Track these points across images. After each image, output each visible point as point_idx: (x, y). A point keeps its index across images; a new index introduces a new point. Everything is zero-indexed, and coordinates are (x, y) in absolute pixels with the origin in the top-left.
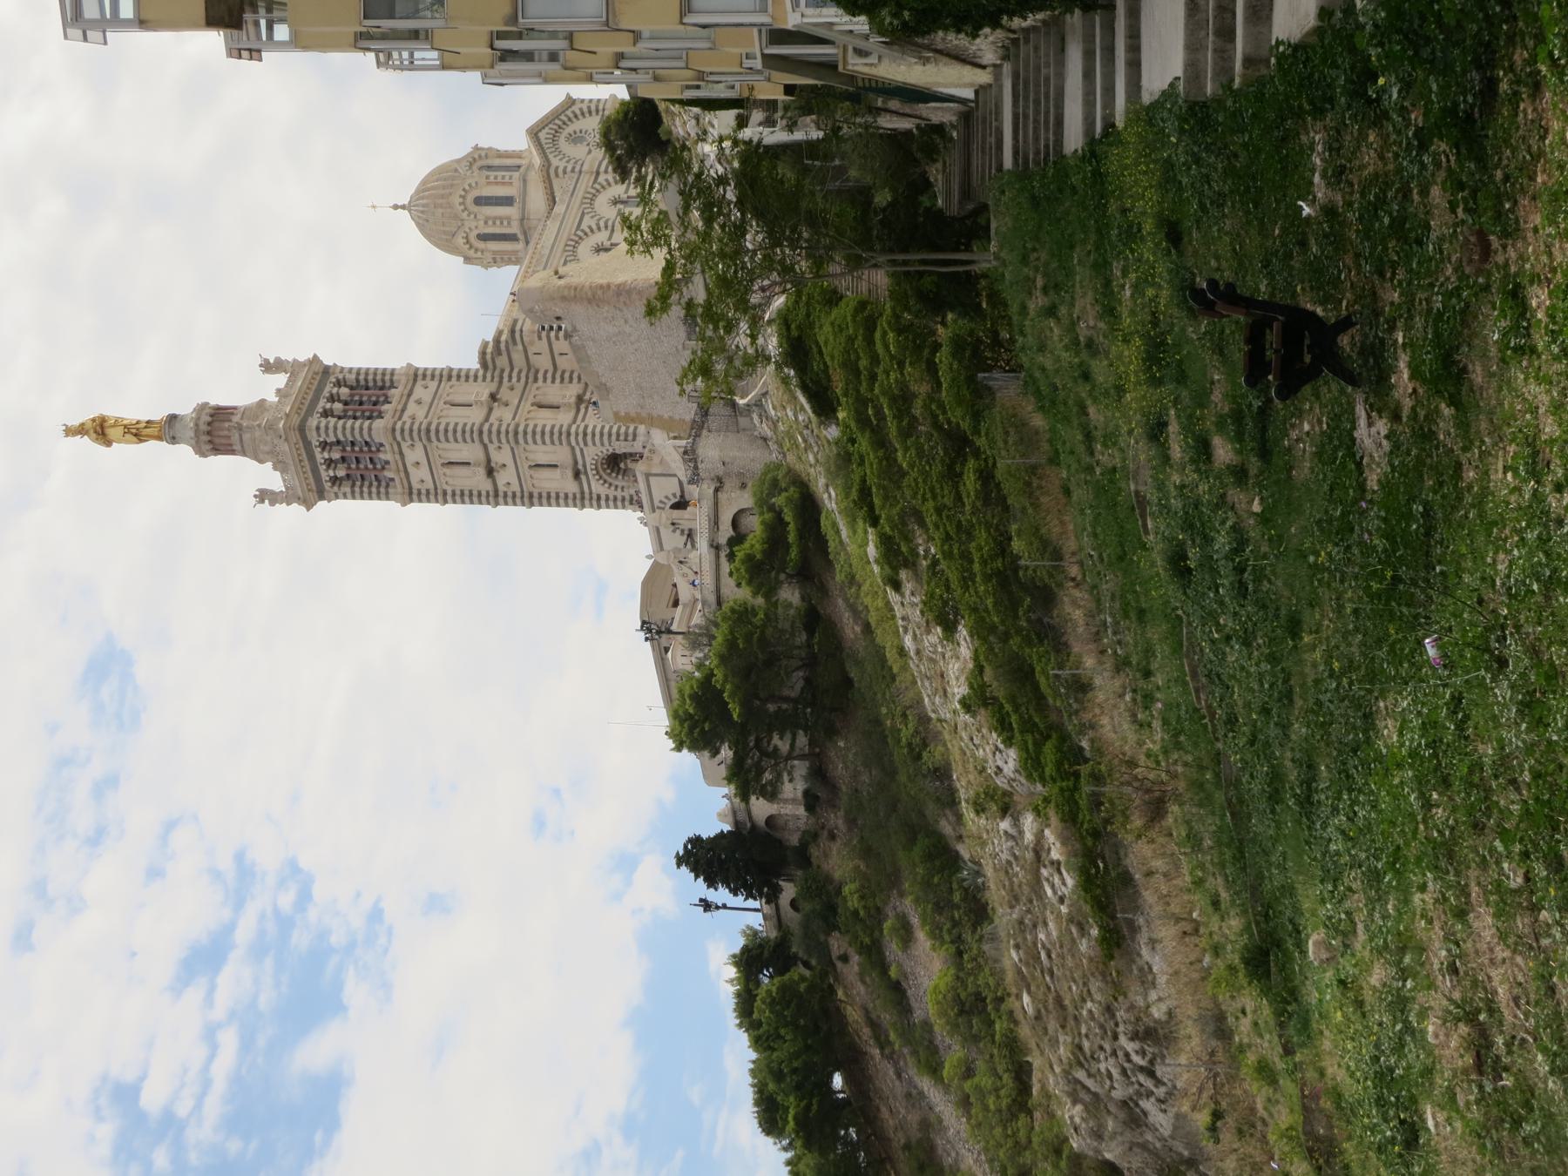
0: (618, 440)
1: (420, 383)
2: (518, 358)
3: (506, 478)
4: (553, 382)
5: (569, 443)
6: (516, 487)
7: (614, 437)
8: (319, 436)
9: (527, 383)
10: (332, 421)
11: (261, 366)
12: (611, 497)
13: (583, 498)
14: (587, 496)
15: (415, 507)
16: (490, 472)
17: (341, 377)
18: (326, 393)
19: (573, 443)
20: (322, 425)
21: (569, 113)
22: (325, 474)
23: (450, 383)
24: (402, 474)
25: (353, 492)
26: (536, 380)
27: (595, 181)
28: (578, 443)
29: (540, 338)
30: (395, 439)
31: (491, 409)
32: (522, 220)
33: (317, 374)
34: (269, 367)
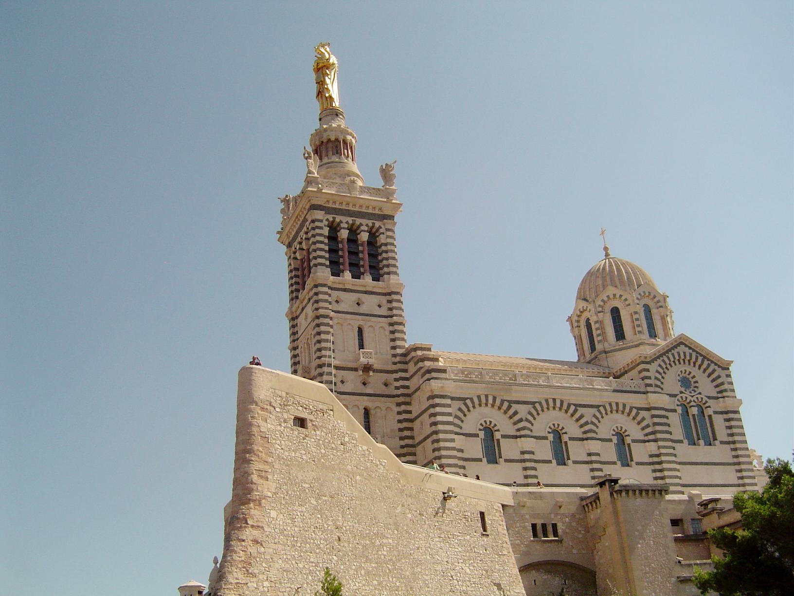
1: (384, 300)
4: (400, 421)
9: (393, 396)
10: (326, 231)
11: (387, 165)
15: (286, 324)
17: (381, 231)
18: (358, 221)
20: (317, 224)
21: (712, 367)
22: (296, 245)
23: (386, 326)
26: (399, 405)
27: (640, 409)
31: (356, 370)
32: (606, 352)
33: (380, 209)
34: (386, 173)
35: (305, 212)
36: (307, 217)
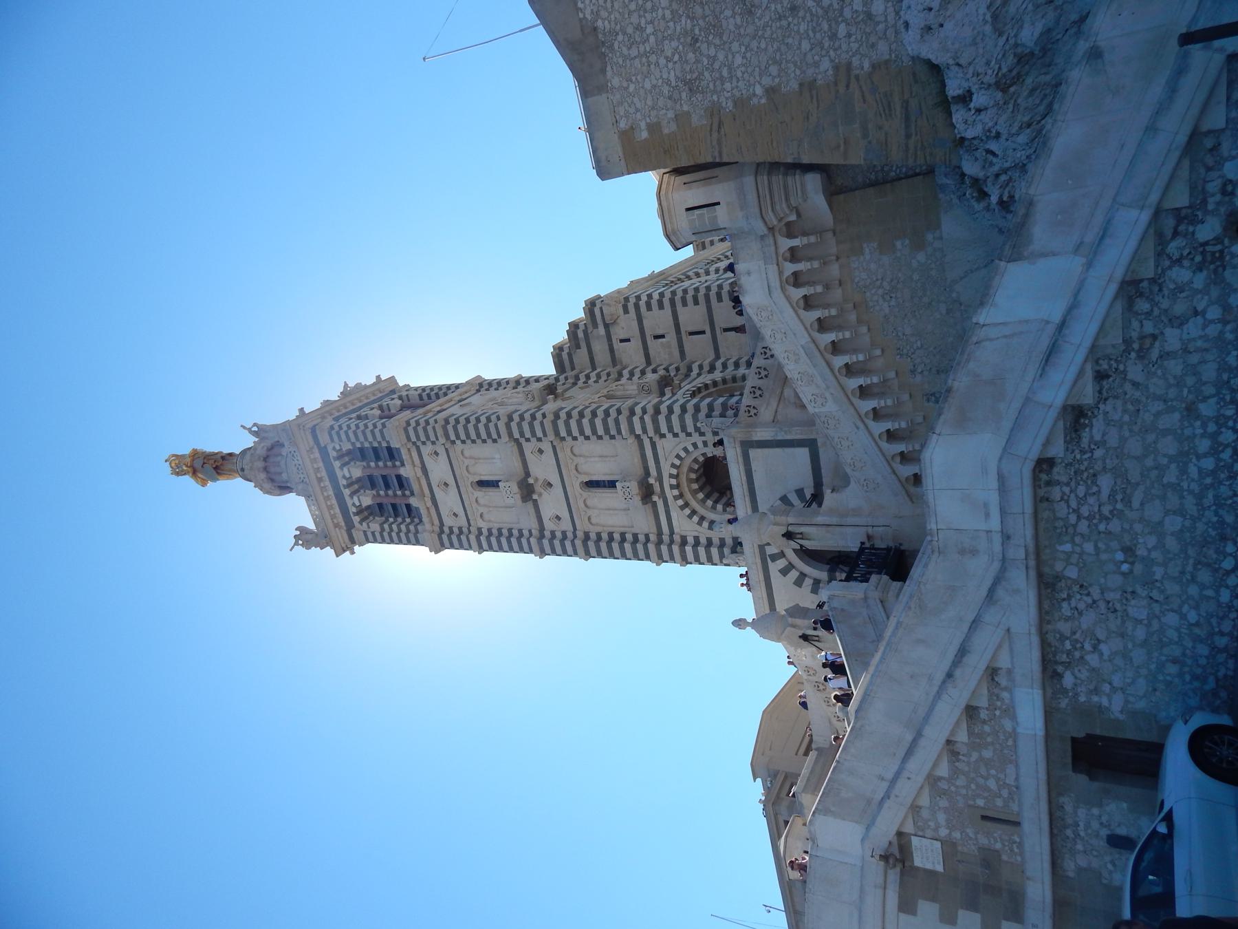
0: (708, 416)
2: (599, 348)
3: (552, 504)
5: (632, 430)
6: (566, 525)
7: (702, 415)
8: (332, 440)
12: (703, 541)
13: (660, 542)
14: (666, 538)
16: (527, 491)
19: (639, 431)
24: (429, 504)
25: (383, 530)
28: (645, 430)
29: (626, 311)
30: (409, 439)
35: (316, 450)
36: (323, 445)
